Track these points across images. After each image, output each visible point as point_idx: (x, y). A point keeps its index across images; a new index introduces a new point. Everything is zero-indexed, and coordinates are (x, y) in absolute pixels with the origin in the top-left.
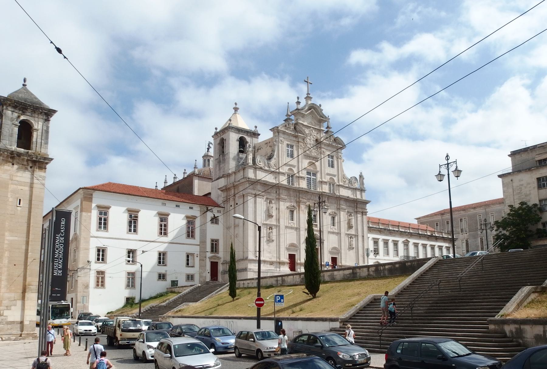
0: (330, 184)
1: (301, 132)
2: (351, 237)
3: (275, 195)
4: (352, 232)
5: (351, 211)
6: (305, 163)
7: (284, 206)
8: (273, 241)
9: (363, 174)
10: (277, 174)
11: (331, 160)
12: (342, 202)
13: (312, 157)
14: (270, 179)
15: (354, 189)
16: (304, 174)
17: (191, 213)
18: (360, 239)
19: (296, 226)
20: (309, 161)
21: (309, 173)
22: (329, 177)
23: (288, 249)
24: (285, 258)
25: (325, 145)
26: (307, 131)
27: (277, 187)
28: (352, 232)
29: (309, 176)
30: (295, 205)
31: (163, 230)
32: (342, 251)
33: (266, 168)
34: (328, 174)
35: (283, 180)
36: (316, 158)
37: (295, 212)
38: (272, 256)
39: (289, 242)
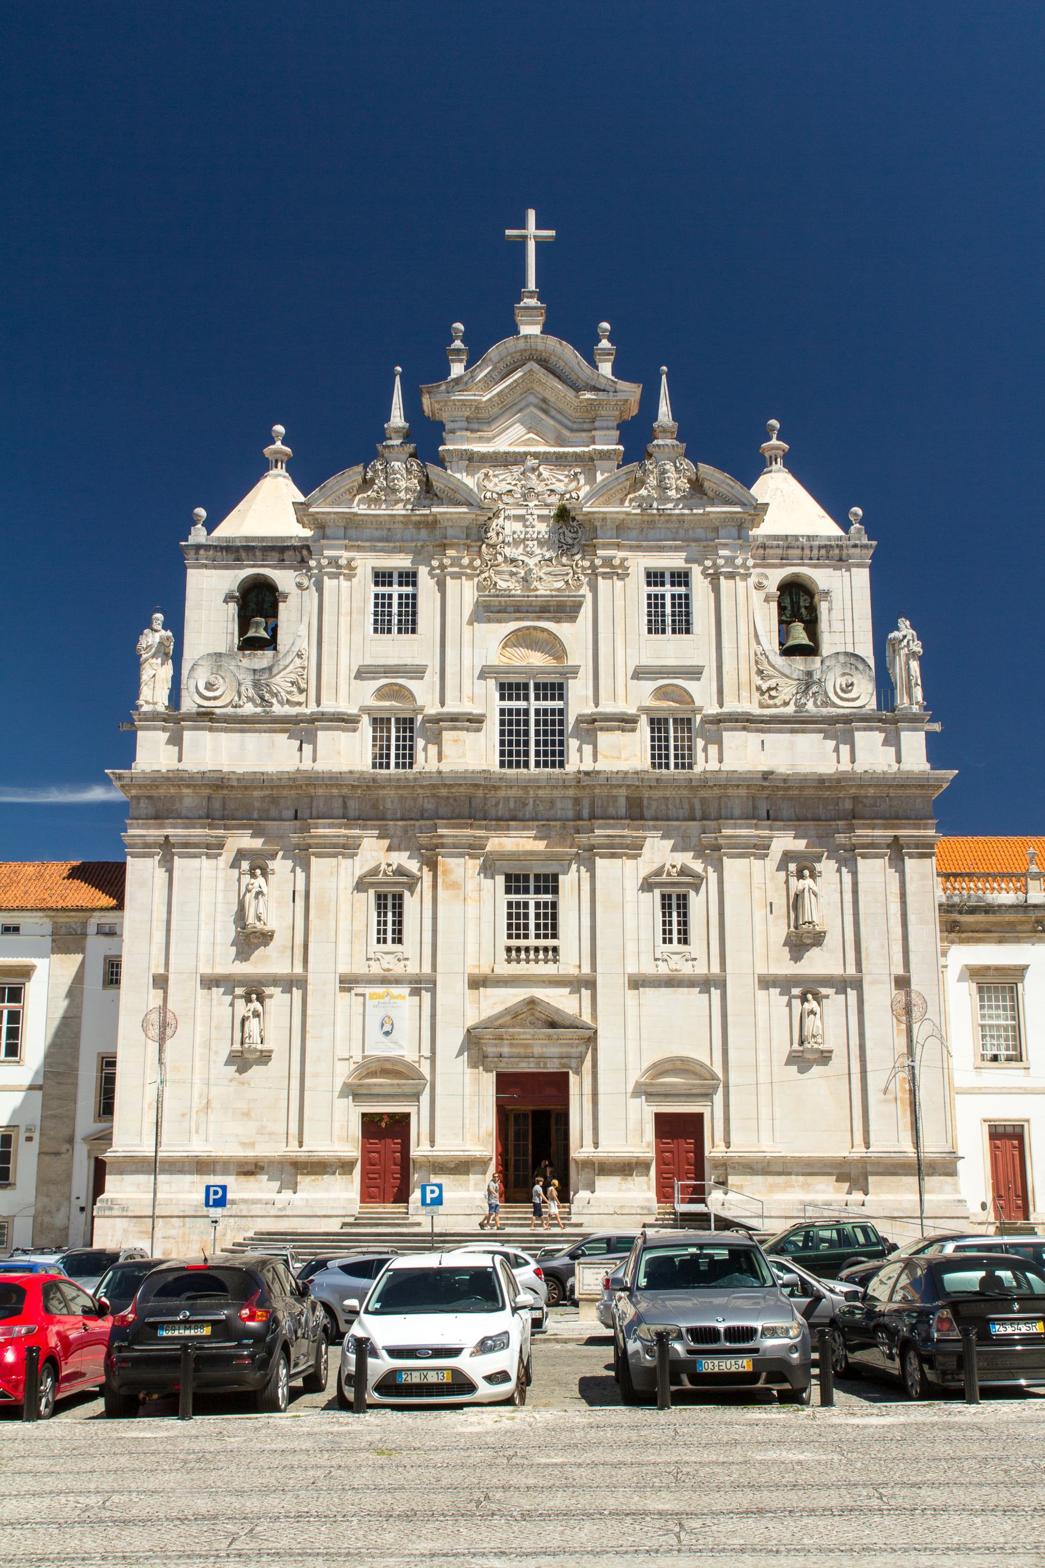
0: (657, 724)
1: (457, 497)
2: (809, 989)
4: (819, 962)
6: (489, 644)
7: (335, 878)
8: (265, 1058)
10: (303, 728)
14: (271, 755)
15: (833, 720)
18: (880, 996)
19: (413, 968)
22: (650, 686)
23: (354, 1092)
24: (338, 1133)
26: (500, 481)
29: (521, 704)
33: (249, 709)
37: (410, 903)
38: (261, 1131)
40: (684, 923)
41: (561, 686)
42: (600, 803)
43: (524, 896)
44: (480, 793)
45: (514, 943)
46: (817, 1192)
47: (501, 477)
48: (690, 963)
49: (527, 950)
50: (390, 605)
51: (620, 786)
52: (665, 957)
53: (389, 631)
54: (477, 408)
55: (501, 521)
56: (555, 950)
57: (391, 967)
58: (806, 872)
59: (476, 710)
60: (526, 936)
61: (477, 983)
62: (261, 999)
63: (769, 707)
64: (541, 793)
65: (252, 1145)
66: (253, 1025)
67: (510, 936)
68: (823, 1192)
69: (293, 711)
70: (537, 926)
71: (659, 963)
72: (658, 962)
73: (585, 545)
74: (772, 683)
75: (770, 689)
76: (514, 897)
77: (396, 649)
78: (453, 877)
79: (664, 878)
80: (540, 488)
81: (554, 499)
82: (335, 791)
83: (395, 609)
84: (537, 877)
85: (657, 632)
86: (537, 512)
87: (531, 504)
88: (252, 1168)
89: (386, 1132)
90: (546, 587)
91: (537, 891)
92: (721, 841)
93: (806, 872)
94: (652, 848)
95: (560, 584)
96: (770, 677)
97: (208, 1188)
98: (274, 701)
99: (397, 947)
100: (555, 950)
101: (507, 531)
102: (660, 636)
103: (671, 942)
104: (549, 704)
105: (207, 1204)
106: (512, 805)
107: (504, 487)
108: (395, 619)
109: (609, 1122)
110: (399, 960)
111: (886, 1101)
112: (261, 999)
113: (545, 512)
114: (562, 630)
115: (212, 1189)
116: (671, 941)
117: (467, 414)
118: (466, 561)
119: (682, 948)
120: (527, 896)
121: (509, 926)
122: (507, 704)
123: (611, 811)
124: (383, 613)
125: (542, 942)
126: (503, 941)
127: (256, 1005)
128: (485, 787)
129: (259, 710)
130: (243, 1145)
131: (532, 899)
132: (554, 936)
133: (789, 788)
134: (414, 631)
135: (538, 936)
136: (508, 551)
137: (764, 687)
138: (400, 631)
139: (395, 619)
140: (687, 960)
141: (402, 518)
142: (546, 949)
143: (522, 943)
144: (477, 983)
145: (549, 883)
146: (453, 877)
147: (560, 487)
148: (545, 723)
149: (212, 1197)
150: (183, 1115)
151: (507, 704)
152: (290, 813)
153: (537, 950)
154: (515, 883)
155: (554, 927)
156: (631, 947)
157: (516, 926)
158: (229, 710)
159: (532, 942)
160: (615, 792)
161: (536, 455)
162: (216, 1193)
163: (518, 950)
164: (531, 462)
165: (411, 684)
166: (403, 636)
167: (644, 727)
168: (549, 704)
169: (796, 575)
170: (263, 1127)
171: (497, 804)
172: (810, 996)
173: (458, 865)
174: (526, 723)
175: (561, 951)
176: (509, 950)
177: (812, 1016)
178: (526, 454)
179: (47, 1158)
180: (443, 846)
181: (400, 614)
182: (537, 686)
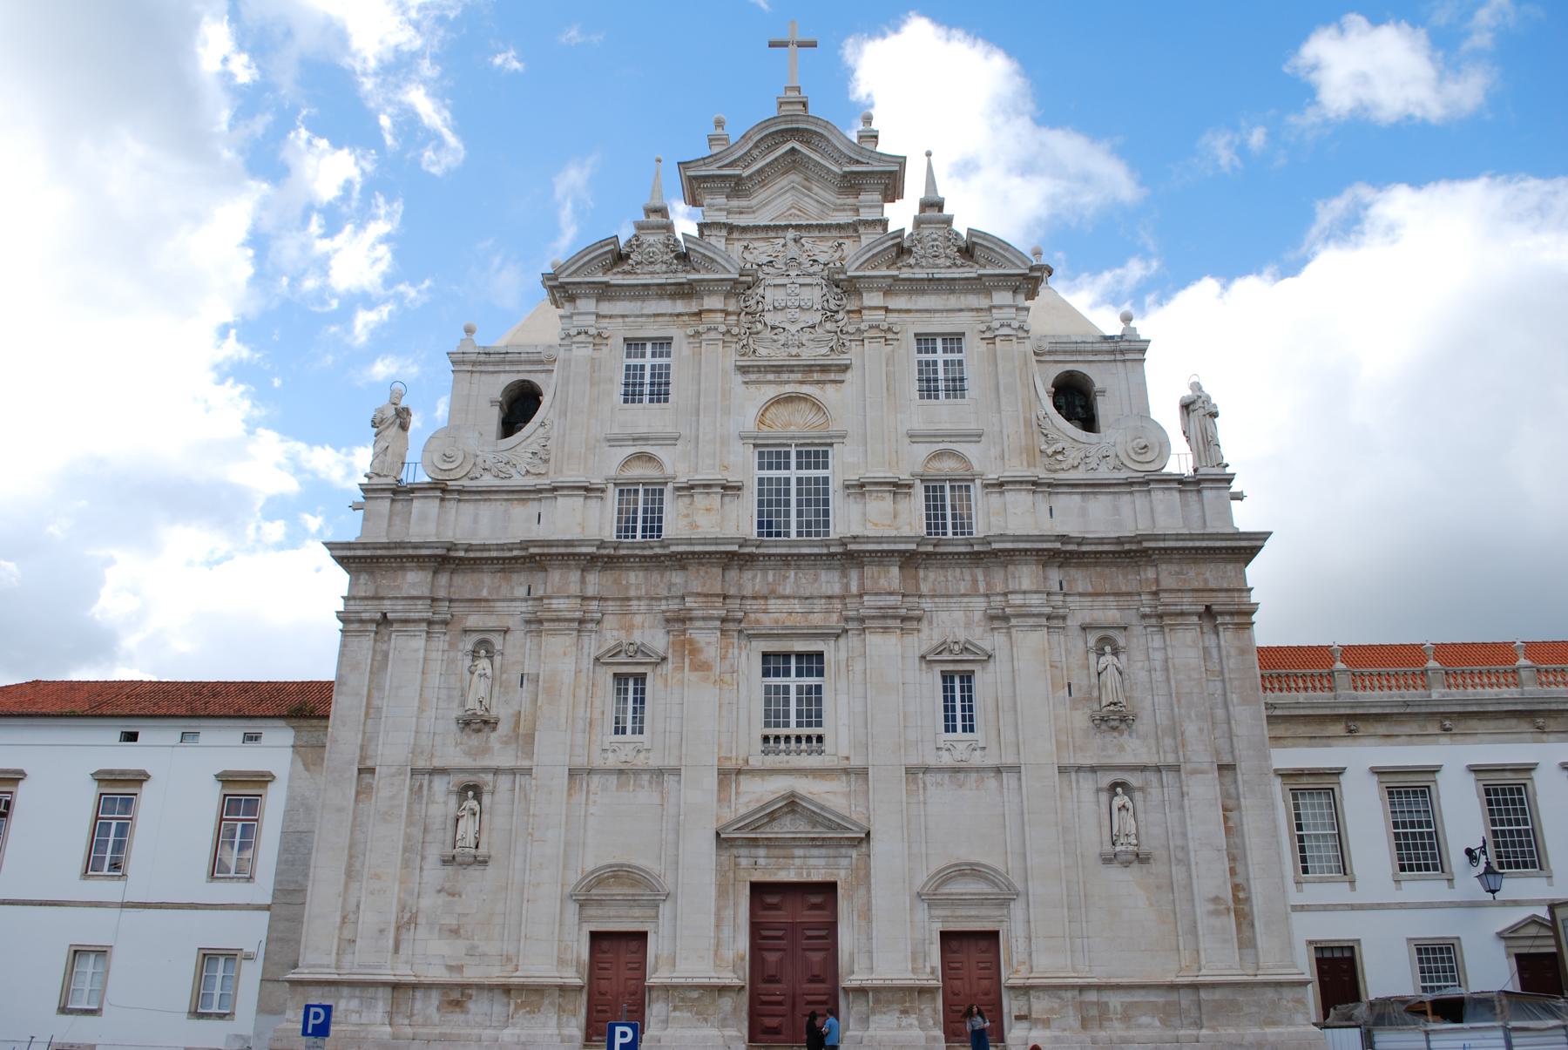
3: (522, 607)
4: (1133, 749)
5: (1109, 613)
9: (1206, 389)
11: (940, 357)
12: (1026, 576)
13: (791, 369)
16: (745, 467)
17: (247, 759)
20: (771, 392)
21: (772, 456)
22: (923, 450)
25: (887, 292)
26: (761, 250)
27: (532, 559)
28: (1133, 749)
30: (658, 640)
31: (107, 848)
32: (1035, 888)
33: (488, 480)
34: (914, 437)
35: (596, 522)
36: (825, 369)
39: (594, 859)
40: (968, 708)
41: (826, 454)
45: (772, 731)
46: (1140, 1026)
48: (978, 752)
49: (788, 738)
50: (642, 376)
53: (641, 401)
55: (760, 291)
56: (820, 739)
58: (1108, 649)
59: (733, 478)
60: (787, 725)
62: (478, 797)
63: (1055, 471)
65: (460, 968)
66: (467, 827)
67: (767, 724)
68: (1147, 1026)
69: (531, 481)
70: (799, 714)
71: (944, 754)
73: (849, 312)
74: (1058, 447)
75: (1056, 453)
77: (646, 417)
78: (703, 657)
79: (945, 656)
80: (804, 259)
81: (816, 268)
83: (647, 379)
84: (800, 656)
86: (801, 280)
87: (793, 273)
88: (456, 995)
89: (618, 951)
90: (813, 353)
91: (799, 674)
92: (1008, 610)
93: (1108, 649)
95: (826, 350)
96: (1056, 441)
97: (308, 1007)
98: (513, 471)
99: (637, 737)
100: (820, 739)
101: (768, 299)
103: (954, 730)
104: (813, 473)
105: (305, 1033)
106: (770, 579)
107: (764, 259)
108: (647, 389)
109: (886, 943)
111: (1216, 913)
112: (478, 797)
113: (808, 280)
114: (828, 395)
115: (313, 1010)
116: (954, 730)
118: (723, 328)
119: (968, 735)
121: (767, 714)
122: (766, 473)
123: (883, 583)
124: (634, 385)
125: (805, 731)
126: (759, 730)
127: (473, 804)
129: (498, 482)
130: (450, 968)
131: (793, 681)
132: (819, 724)
133: (1084, 553)
134: (666, 400)
135: (799, 724)
136: (769, 318)
137: (1050, 451)
138: (651, 401)
139: (647, 389)
142: (809, 739)
143: (782, 731)
145: (813, 662)
146: (703, 657)
147: (822, 258)
148: (808, 492)
149: (312, 1022)
150: (381, 931)
151: (766, 473)
152: (521, 592)
153: (798, 739)
154: (773, 663)
155: (819, 715)
157: (774, 715)
158: (466, 482)
159: (793, 730)
161: (798, 227)
162: (317, 1016)
163: (777, 738)
164: (791, 234)
166: (656, 405)
167: (919, 491)
168: (813, 473)
169: (1070, 374)
170: (474, 947)
171: (754, 578)
172: (1119, 790)
173: (709, 643)
174: (787, 492)
175: (827, 740)
176: (766, 739)
177: (1124, 812)
178: (787, 227)
179: (269, 985)
180: (691, 619)
181: (652, 384)
182: (799, 454)
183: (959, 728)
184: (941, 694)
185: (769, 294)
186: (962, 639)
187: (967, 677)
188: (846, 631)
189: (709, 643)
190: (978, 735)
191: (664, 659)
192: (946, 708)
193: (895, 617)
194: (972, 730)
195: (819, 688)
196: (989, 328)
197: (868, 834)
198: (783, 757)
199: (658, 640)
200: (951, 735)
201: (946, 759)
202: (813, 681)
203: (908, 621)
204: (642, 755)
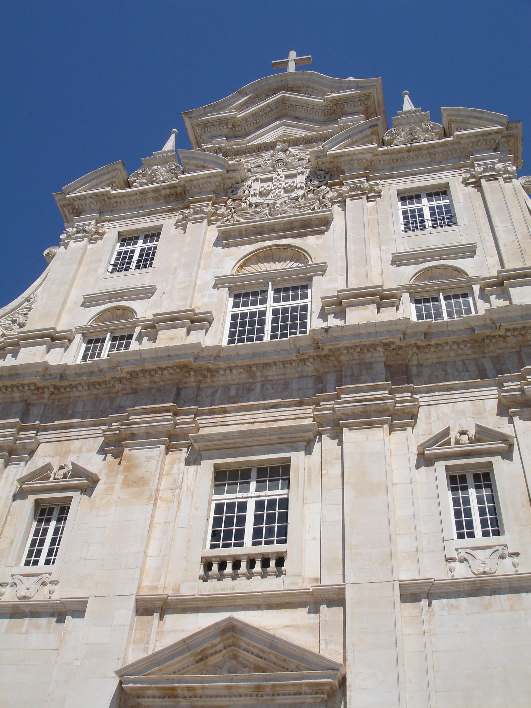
30: (94, 463)
42: (349, 373)
43: (240, 495)
44: (192, 380)
47: (251, 162)
48: (508, 561)
51: (374, 346)
52: (463, 554)
54: (234, 126)
55: (248, 183)
57: (28, 594)
61: (151, 607)
64: (271, 373)
71: (456, 565)
72: (452, 564)
76: (226, 498)
78: (139, 473)
82: (17, 395)
85: (415, 229)
94: (428, 417)
102: (420, 232)
103: (471, 535)
110: (44, 584)
114: (310, 243)
116: (471, 535)
117: (225, 131)
120: (245, 495)
128: (198, 371)
140: (502, 557)
141: (152, 194)
144: (151, 607)
146: (139, 473)
156: (404, 544)
160: (368, 357)
165: (134, 305)
173: (149, 458)
183: (478, 529)
184: (453, 520)
185: (257, 186)
186: (472, 432)
187: (485, 479)
188: (320, 434)
189: (149, 458)
190: (510, 538)
191: (94, 481)
192: (457, 514)
193: (381, 412)
194: (497, 533)
195: (284, 503)
196: (473, 176)
197: (343, 681)
198: (228, 582)
199: (94, 463)
200: (466, 542)
201: (461, 572)
202: (278, 494)
203: (402, 418)
204: (46, 589)
